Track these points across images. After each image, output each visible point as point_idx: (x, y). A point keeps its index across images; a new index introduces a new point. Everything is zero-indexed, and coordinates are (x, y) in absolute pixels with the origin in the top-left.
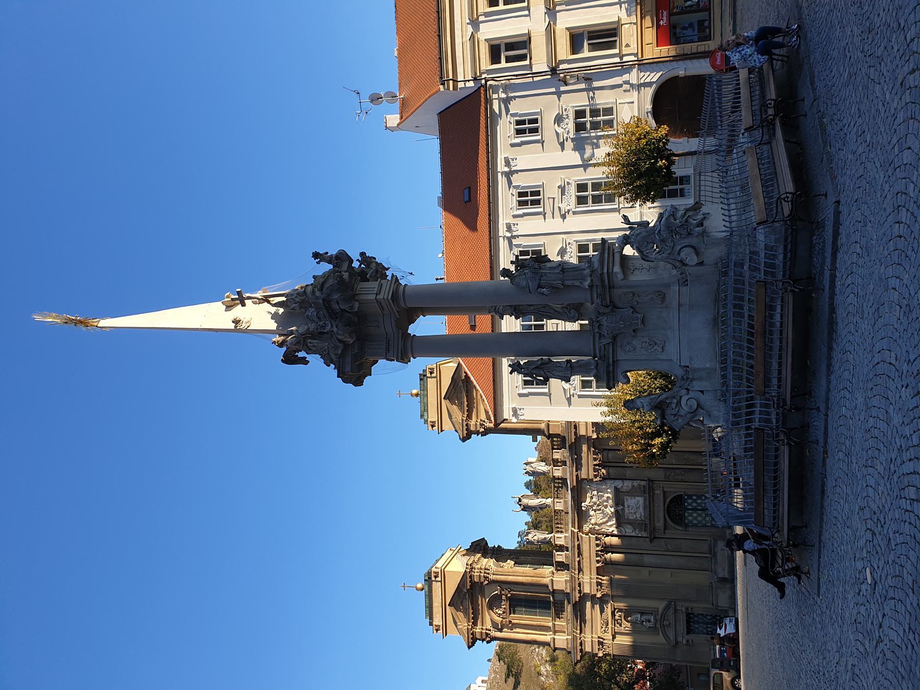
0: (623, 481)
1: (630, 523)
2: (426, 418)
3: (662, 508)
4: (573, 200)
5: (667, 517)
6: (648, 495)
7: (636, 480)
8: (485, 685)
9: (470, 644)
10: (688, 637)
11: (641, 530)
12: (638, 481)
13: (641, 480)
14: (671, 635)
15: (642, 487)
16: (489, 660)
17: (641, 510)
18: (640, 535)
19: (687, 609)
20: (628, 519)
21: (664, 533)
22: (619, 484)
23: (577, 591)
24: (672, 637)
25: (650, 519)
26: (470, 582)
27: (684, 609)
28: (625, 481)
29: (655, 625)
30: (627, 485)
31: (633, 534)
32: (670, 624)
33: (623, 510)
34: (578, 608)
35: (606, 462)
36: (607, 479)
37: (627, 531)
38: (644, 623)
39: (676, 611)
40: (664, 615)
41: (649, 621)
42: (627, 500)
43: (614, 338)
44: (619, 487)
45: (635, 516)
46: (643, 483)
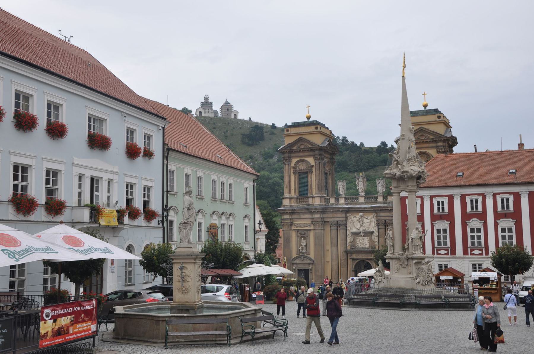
0: (377, 236)
1: (354, 240)
3: (364, 258)
5: (359, 260)
6: (370, 250)
8: (233, 117)
9: (281, 151)
10: (297, 269)
11: (351, 246)
12: (378, 245)
13: (379, 246)
14: (298, 261)
15: (374, 247)
16: (250, 119)
17: (362, 246)
19: (311, 270)
21: (351, 259)
22: (376, 234)
24: (296, 261)
25: (357, 251)
26: (314, 149)
27: (310, 268)
28: (377, 238)
29: (300, 253)
31: (348, 242)
32: (302, 261)
33: (361, 236)
34: (306, 211)
36: (378, 227)
37: (350, 238)
39: (309, 264)
40: (306, 257)
42: (367, 238)
43: (399, 259)
44: (374, 234)
45: (358, 242)
46: (377, 247)
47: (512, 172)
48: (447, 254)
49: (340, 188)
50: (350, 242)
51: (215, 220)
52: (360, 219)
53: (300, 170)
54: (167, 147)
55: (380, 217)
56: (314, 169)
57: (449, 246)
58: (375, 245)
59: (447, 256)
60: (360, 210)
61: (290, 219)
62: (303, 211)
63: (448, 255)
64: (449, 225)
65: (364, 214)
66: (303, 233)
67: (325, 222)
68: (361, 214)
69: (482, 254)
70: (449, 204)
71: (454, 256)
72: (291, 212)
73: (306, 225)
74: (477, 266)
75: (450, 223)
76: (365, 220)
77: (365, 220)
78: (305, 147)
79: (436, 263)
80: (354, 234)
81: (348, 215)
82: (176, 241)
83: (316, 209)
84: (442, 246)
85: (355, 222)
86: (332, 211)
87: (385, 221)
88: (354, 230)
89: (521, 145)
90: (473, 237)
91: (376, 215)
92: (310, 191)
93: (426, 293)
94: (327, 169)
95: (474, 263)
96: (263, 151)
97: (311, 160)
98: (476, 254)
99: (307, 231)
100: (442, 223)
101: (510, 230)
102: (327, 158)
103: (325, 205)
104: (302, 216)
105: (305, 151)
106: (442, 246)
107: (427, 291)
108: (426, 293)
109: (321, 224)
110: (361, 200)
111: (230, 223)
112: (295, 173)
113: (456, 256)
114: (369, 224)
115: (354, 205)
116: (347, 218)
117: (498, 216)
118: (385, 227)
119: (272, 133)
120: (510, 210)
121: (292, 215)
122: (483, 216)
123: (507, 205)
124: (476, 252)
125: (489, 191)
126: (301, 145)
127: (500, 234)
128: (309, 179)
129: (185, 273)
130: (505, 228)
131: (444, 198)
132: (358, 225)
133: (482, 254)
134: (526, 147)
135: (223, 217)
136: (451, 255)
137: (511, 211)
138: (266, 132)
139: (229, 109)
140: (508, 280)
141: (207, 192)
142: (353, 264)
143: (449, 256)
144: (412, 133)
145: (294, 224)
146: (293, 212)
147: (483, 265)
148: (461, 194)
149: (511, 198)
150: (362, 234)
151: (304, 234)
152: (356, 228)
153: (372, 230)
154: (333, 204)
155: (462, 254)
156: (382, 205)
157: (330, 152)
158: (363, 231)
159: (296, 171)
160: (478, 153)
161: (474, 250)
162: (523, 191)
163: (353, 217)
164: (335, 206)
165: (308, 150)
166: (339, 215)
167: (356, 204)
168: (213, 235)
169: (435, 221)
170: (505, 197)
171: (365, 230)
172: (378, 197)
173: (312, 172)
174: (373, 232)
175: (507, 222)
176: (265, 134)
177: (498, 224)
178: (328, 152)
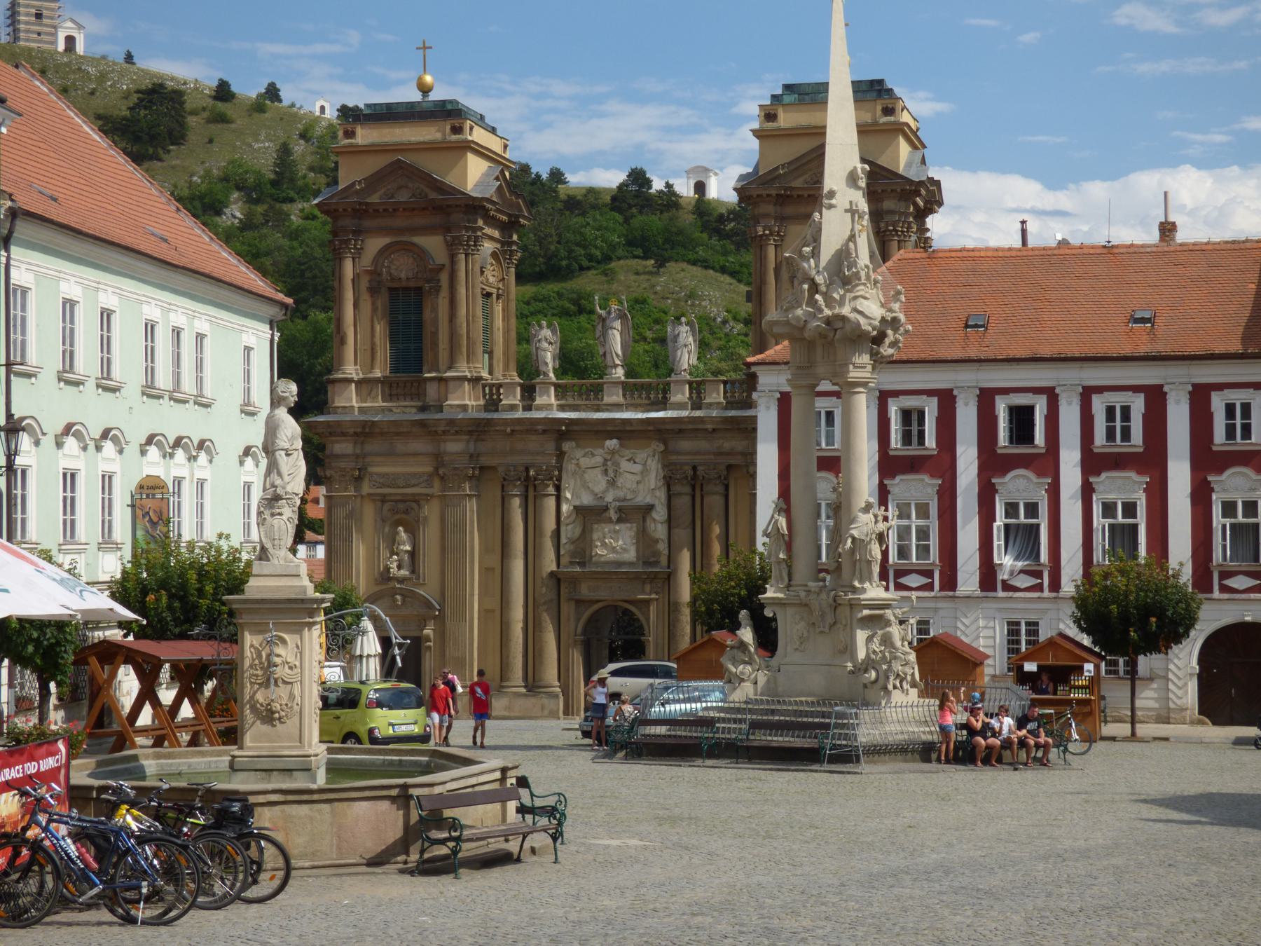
1: (585, 534)
2: (787, 99)
4: (1111, 497)
7: (669, 547)
8: (61, 46)
12: (666, 552)
13: (669, 557)
15: (652, 560)
18: (562, 553)
20: (591, 531)
22: (660, 514)
23: (447, 428)
26: (449, 206)
30: (659, 530)
33: (610, 521)
35: (702, 490)
36: (669, 489)
37: (570, 527)
38: (395, 557)
41: (399, 567)
44: (654, 515)
47: (1143, 318)
48: (929, 587)
49: (537, 349)
50: (572, 542)
51: (154, 465)
52: (606, 460)
53: (393, 279)
54: (9, 204)
55: (678, 453)
56: (444, 278)
57: (937, 562)
58: (657, 554)
59: (926, 594)
60: (609, 428)
61: (357, 456)
62: (405, 430)
65: (621, 445)
66: (401, 506)
67: (482, 468)
68: (612, 443)
70: (940, 421)
71: (951, 593)
72: (359, 430)
73: (413, 482)
74: (1023, 628)
76: (625, 465)
77: (625, 465)
78: (413, 195)
80: (579, 510)
81: (567, 446)
82: (34, 540)
83: (451, 422)
85: (589, 471)
86: (509, 430)
87: (694, 468)
88: (586, 500)
89: (1167, 229)
91: (662, 448)
92: (428, 356)
93: (894, 715)
94: (491, 279)
95: (1014, 617)
96: (182, 184)
97: (433, 244)
99: (417, 502)
100: (914, 483)
101: (1130, 509)
102: (492, 238)
103: (487, 408)
104: (400, 446)
105: (413, 209)
107: (899, 709)
108: (894, 715)
109: (471, 478)
110: (614, 396)
111: (199, 474)
112: (373, 291)
114: (638, 478)
115: (584, 411)
116: (561, 455)
117: (1093, 463)
118: (694, 489)
119: (221, 119)
120: (1133, 442)
121: (362, 443)
122: (1048, 464)
123: (1122, 427)
125: (1069, 379)
126: (400, 188)
127: (1098, 520)
128: (427, 314)
129: (278, 656)
130: (1115, 504)
132: (598, 481)
133: (1039, 588)
134: (1183, 236)
135: (180, 454)
136: (941, 589)
137: (1135, 446)
138: (194, 113)
139: (45, 12)
140: (1116, 672)
141: (128, 369)
142: (578, 620)
144: (859, 188)
145: (371, 474)
146: (367, 430)
147: (1041, 623)
148: (981, 389)
149: (1138, 405)
150: (613, 514)
151: (407, 512)
152: (592, 492)
153: (648, 500)
154: (513, 408)
156: (684, 413)
157: (505, 218)
158: (618, 504)
159: (379, 282)
160: (1032, 249)
162: (1174, 383)
163: (583, 452)
164: (520, 414)
165: (424, 209)
166: (533, 443)
167: (598, 409)
168: (151, 520)
169: (893, 477)
170: (1118, 399)
171: (625, 500)
172: (672, 385)
173: (437, 290)
174: (650, 508)
176: (192, 121)
177: (1093, 490)
178: (493, 218)
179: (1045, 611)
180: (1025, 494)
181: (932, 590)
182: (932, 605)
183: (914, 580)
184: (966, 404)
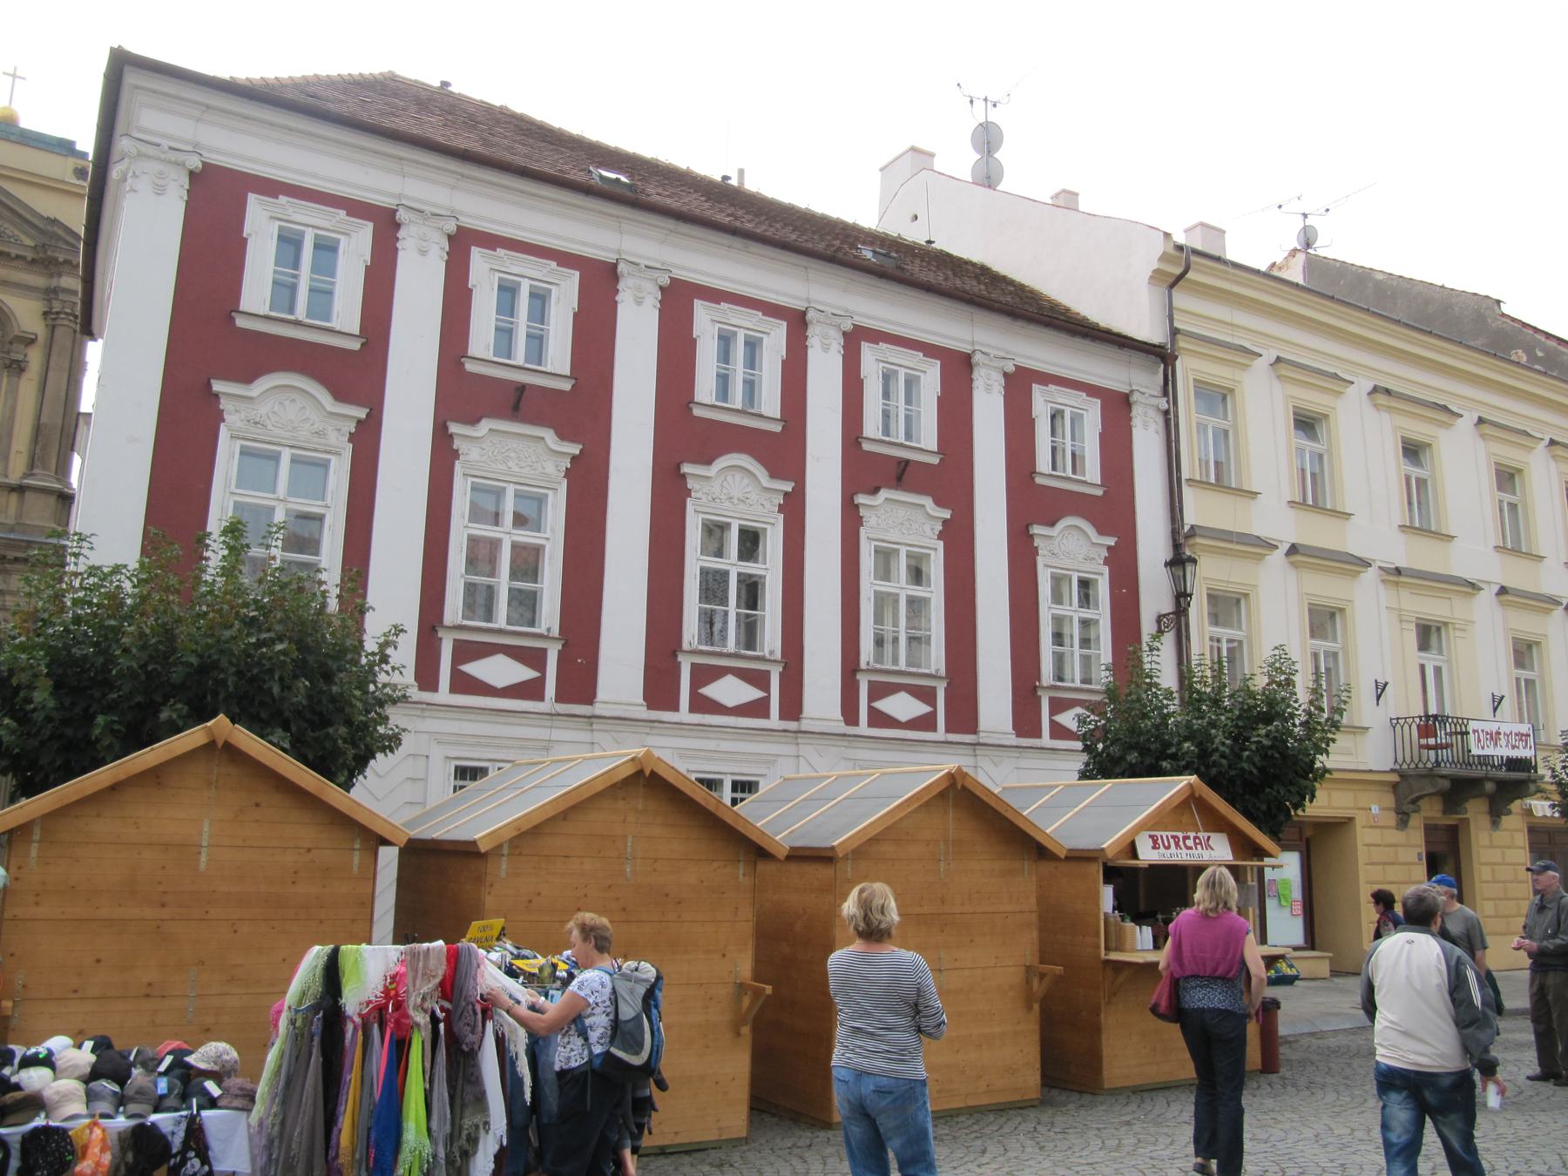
48: (531, 690)
63: (540, 697)
64: (568, 473)
69: (757, 709)
75: (574, 459)
79: (437, 753)
84: (501, 621)
90: (713, 585)
98: (730, 702)
106: (501, 621)
113: (598, 709)
124: (730, 691)
131: (552, 271)
133: (757, 709)
136: (560, 698)
143: (549, 702)
155: (640, 700)
161: (717, 673)
175: (902, 512)
179: (771, 760)
180: (741, 506)
181: (541, 698)
182: (542, 733)
183: (499, 670)
184: (639, 302)
